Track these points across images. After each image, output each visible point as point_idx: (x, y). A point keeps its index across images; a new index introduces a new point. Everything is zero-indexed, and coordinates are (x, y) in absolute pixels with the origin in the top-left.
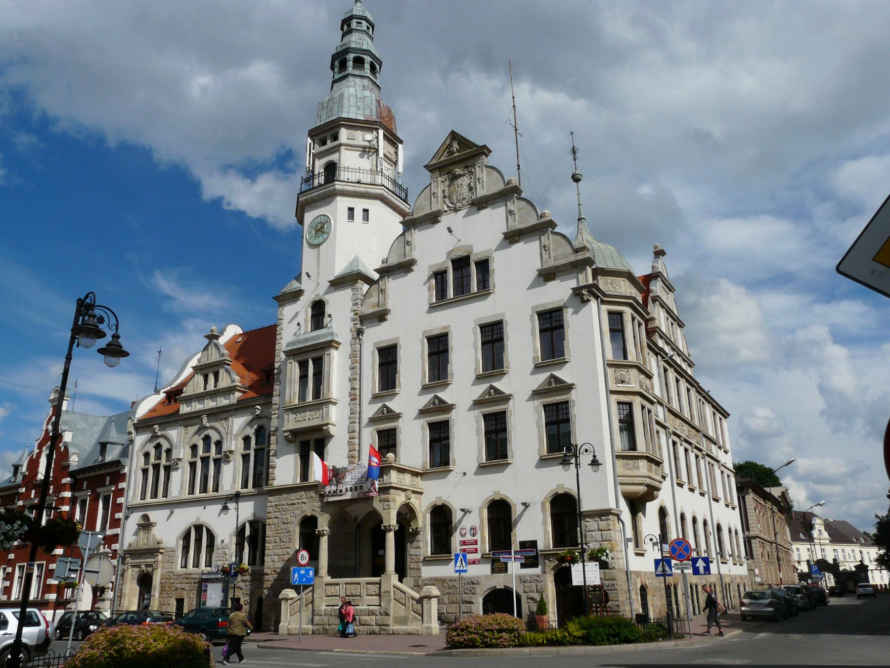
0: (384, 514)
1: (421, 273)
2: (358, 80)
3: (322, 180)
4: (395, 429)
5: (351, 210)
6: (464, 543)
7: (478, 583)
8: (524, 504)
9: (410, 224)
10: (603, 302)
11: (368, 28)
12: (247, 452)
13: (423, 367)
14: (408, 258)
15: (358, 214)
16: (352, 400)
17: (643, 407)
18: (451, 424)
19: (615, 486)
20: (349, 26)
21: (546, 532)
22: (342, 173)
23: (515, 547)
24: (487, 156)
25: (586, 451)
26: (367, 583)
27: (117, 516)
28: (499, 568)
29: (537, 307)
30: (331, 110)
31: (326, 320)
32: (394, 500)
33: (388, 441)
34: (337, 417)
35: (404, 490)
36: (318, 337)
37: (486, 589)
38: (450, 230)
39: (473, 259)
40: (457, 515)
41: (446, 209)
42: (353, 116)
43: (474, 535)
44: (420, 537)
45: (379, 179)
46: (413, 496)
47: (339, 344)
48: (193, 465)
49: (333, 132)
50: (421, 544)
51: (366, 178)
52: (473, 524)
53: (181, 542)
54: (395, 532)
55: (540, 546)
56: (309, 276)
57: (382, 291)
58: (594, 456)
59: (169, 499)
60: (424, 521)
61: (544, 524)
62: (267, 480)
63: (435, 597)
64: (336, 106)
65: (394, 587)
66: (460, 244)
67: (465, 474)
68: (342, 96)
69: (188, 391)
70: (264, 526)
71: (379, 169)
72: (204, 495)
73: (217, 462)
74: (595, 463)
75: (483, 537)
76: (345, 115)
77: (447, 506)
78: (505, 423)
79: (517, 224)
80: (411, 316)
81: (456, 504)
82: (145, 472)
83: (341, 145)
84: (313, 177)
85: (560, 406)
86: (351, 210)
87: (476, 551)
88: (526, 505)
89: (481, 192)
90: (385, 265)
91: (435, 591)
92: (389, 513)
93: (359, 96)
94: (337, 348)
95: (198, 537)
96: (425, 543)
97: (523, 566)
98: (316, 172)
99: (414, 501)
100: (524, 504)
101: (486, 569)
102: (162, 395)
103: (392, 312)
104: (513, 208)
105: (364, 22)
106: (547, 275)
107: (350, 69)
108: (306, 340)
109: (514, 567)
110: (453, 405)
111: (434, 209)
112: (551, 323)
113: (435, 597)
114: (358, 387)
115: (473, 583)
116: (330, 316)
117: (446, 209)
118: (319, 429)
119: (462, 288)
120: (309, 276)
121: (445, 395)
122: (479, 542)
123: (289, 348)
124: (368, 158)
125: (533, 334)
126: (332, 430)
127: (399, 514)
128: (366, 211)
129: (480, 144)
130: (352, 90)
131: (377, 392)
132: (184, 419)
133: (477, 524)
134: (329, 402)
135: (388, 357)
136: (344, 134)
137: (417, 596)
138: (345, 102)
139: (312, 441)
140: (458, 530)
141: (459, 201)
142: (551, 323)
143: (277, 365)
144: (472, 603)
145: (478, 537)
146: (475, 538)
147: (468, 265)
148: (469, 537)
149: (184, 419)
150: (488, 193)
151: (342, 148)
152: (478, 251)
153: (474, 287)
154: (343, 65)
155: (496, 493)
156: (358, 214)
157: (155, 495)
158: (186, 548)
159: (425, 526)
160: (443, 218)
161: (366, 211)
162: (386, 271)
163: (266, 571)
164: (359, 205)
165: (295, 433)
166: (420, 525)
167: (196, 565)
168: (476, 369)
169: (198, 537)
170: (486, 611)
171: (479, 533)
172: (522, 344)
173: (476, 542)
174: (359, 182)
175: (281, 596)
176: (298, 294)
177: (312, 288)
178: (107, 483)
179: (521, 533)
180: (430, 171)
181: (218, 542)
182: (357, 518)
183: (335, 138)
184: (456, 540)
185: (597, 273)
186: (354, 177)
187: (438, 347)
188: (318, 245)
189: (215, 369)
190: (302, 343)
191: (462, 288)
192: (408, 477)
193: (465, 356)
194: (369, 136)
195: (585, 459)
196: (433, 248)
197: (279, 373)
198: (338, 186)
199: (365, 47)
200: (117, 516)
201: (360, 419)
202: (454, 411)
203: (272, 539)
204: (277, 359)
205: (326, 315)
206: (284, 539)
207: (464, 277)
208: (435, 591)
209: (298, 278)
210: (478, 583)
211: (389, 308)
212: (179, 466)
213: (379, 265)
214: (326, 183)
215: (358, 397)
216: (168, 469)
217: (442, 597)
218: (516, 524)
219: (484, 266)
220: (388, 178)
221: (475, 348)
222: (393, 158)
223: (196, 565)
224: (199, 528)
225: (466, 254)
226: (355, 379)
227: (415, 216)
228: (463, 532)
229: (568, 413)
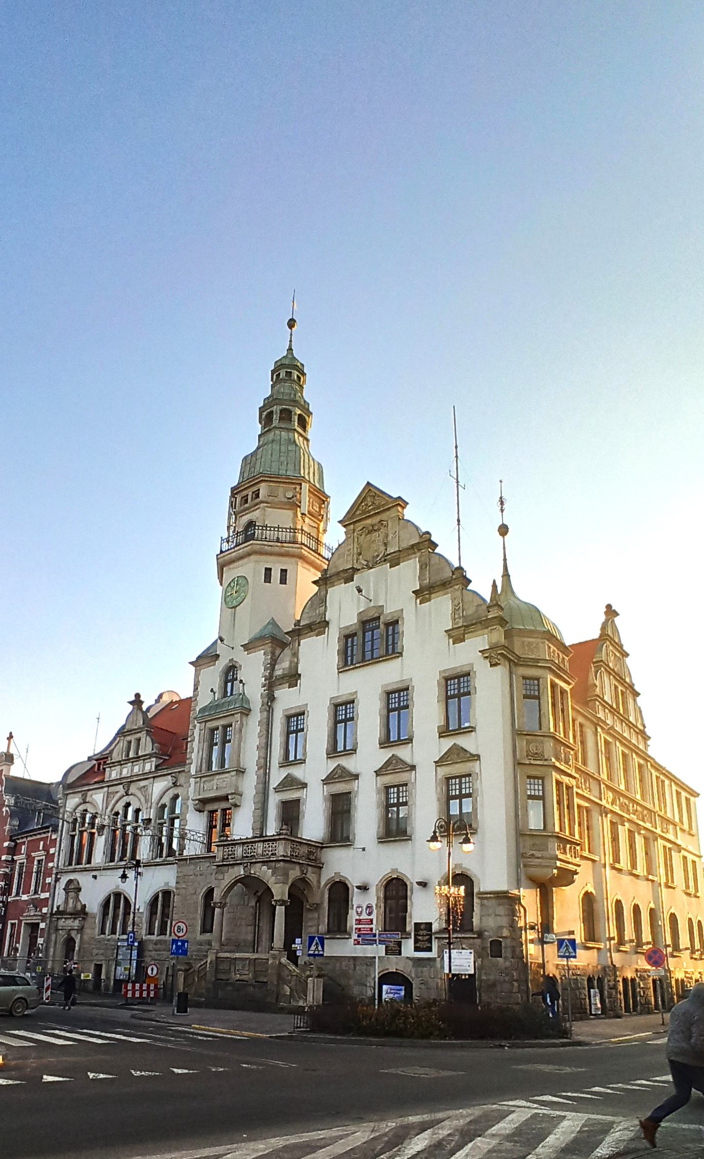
1: (333, 637)
4: (297, 802)
5: (268, 571)
6: (359, 922)
9: (324, 582)
10: (516, 665)
11: (299, 378)
15: (276, 575)
17: (559, 783)
18: (352, 795)
19: (518, 866)
20: (278, 375)
23: (410, 927)
24: (403, 508)
27: (48, 880)
28: (395, 950)
29: (444, 671)
33: (291, 813)
38: (360, 591)
43: (370, 914)
46: (310, 869)
49: (255, 488)
55: (435, 927)
57: (295, 654)
59: (93, 864)
64: (258, 462)
66: (372, 604)
67: (364, 849)
69: (116, 757)
81: (354, 881)
83: (262, 502)
86: (268, 571)
95: (117, 903)
97: (417, 949)
99: (311, 876)
101: (379, 950)
106: (457, 635)
107: (275, 423)
109: (408, 948)
112: (456, 687)
118: (225, 798)
121: (350, 764)
122: (374, 922)
128: (284, 572)
129: (395, 496)
132: (108, 786)
135: (295, 722)
142: (456, 687)
145: (374, 917)
146: (370, 917)
148: (364, 916)
149: (108, 786)
152: (390, 610)
154: (270, 416)
155: (394, 871)
156: (276, 575)
157: (79, 862)
158: (105, 913)
161: (284, 572)
162: (299, 632)
165: (204, 802)
169: (117, 903)
171: (375, 911)
172: (426, 712)
173: (371, 920)
174: (278, 540)
178: (41, 848)
180: (345, 526)
182: (257, 892)
184: (352, 916)
185: (508, 635)
187: (343, 712)
188: (235, 607)
189: (138, 735)
196: (345, 608)
200: (48, 880)
213: (291, 627)
223: (113, 932)
224: (118, 895)
225: (377, 615)
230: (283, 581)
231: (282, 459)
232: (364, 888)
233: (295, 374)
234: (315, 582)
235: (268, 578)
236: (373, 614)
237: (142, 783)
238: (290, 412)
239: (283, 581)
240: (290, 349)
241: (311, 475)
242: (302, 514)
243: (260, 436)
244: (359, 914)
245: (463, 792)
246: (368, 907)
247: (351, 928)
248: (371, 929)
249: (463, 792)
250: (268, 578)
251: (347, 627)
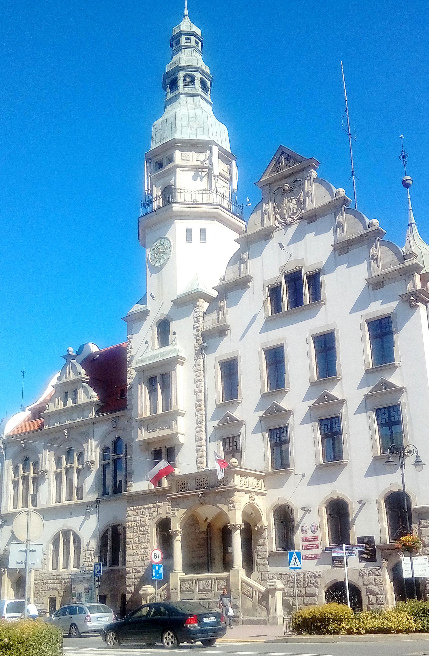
0: (230, 514)
2: (189, 99)
3: (161, 203)
6: (306, 540)
7: (320, 577)
8: (359, 502)
11: (197, 43)
12: (106, 462)
13: (262, 377)
14: (243, 275)
16: (198, 411)
21: (381, 528)
22: (179, 194)
23: (353, 541)
25: (410, 452)
26: (218, 579)
30: (165, 132)
31: (171, 337)
32: (239, 502)
34: (184, 429)
35: (248, 492)
36: (165, 354)
37: (327, 582)
39: (304, 271)
40: (298, 515)
41: (277, 225)
42: (186, 136)
43: (314, 532)
44: (265, 534)
45: (214, 199)
47: (184, 359)
48: (58, 476)
50: (267, 542)
51: (201, 198)
52: (314, 523)
53: (51, 546)
54: (242, 531)
56: (153, 297)
58: (417, 457)
60: (268, 521)
61: (380, 521)
62: (126, 487)
63: (279, 590)
65: (243, 581)
66: (292, 258)
68: (174, 117)
70: (125, 528)
71: (213, 187)
72: (69, 502)
73: (79, 471)
74: (418, 463)
75: (322, 534)
76: (178, 136)
77: (289, 506)
78: (339, 427)
79: (346, 234)
80: (248, 329)
82: (15, 484)
84: (151, 201)
85: (392, 410)
87: (317, 547)
88: (362, 504)
89: (311, 205)
90: (223, 282)
91: (279, 584)
92: (235, 514)
93: (191, 115)
94: (182, 364)
96: (270, 541)
98: (155, 196)
100: (359, 502)
102: (27, 414)
103: (231, 327)
104: (341, 220)
105: (192, 38)
107: (181, 89)
108: (154, 357)
110: (290, 411)
111: (267, 224)
113: (279, 590)
114: (203, 398)
115: (315, 577)
116: (174, 333)
117: (277, 225)
119: (296, 300)
120: (153, 297)
123: (139, 365)
124: (201, 180)
125: (363, 342)
126: (182, 439)
127: (244, 513)
130: (184, 110)
131: (221, 402)
133: (316, 521)
134: (177, 413)
136: (179, 157)
137: (263, 589)
138: (178, 122)
139: (165, 451)
140: (300, 528)
141: (289, 216)
143: (129, 381)
144: (316, 595)
145: (318, 534)
146: (316, 535)
147: (301, 278)
148: (309, 534)
150: (317, 206)
151: (178, 170)
152: (310, 264)
153: (307, 299)
158: (56, 551)
159: (269, 524)
160: (275, 235)
163: (128, 569)
164: (196, 225)
166: (265, 523)
167: (66, 566)
168: (311, 376)
170: (327, 601)
173: (316, 539)
175: (141, 592)
176: (146, 313)
177: (157, 308)
179: (359, 529)
181: (84, 545)
183: (171, 160)
186: (190, 198)
190: (150, 360)
191: (296, 300)
192: (251, 480)
193: (301, 366)
194: (202, 156)
195: (409, 460)
197: (131, 388)
198: (176, 208)
199: (194, 64)
201: (206, 428)
202: (291, 417)
203: (132, 540)
204: (128, 376)
205: (171, 333)
206: (143, 541)
207: (298, 290)
208: (279, 584)
209: (143, 301)
210: (320, 577)
211: (228, 323)
212: (46, 477)
213: (216, 283)
214: (163, 206)
215: (203, 408)
216: (36, 480)
217: (287, 590)
218: (354, 520)
219: (314, 279)
220: (223, 196)
221: (310, 358)
222: (227, 175)
224: (66, 533)
226: (200, 391)
227: (248, 234)
228: (305, 529)
229: (398, 416)
231: (191, 123)
232: (307, 511)
234: (237, 241)
236: (292, 267)
237: (83, 429)
238: (193, 78)
241: (219, 137)
242: (215, 176)
244: (304, 532)
245: (393, 420)
246: (312, 526)
247: (298, 545)
248: (317, 545)
249: (393, 420)
251: (271, 280)
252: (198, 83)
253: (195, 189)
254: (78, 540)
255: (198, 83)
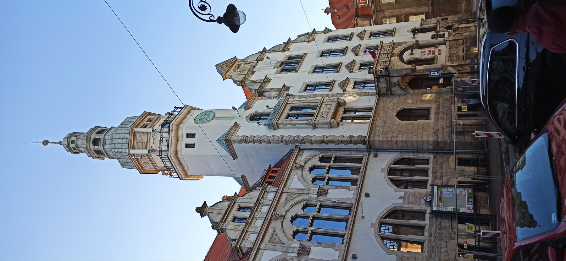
5: (187, 146)
15: (190, 141)
86: (187, 146)
107: (100, 148)
128: (188, 136)
154: (98, 152)
156: (190, 141)
161: (188, 136)
174: (168, 141)
230: (193, 136)
233: (73, 139)
235: (192, 146)
239: (193, 136)
240: (60, 143)
243: (109, 158)
250: (192, 146)
252: (98, 136)
253: (160, 140)
254: (393, 213)
255: (98, 136)
